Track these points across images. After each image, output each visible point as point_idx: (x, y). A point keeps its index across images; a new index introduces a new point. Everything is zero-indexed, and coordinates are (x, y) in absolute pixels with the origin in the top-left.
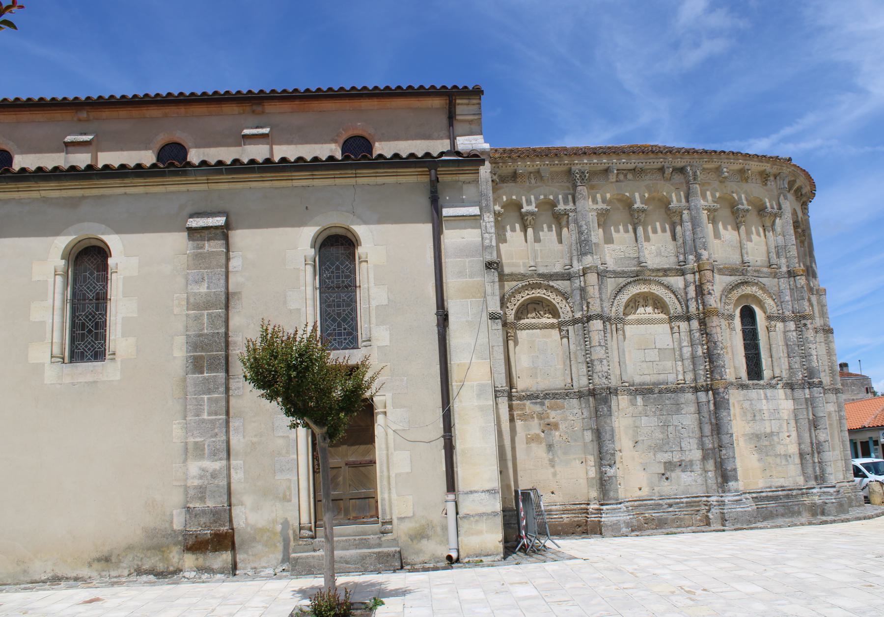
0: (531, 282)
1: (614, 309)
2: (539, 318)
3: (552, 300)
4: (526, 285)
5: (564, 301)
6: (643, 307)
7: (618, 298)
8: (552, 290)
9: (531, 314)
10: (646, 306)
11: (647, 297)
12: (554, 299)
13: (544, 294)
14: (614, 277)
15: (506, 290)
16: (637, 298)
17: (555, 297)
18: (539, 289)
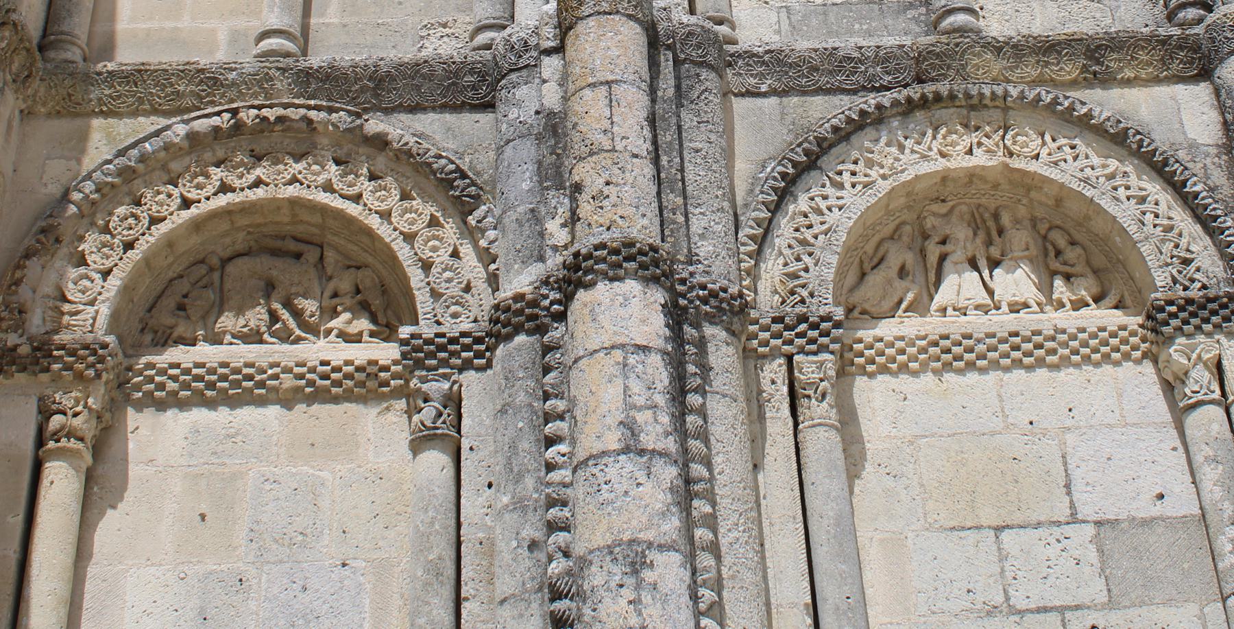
0: (247, 116)
1: (772, 269)
2: (286, 337)
3: (374, 222)
4: (216, 129)
5: (450, 230)
6: (973, 263)
7: (803, 203)
8: (381, 162)
9: (240, 311)
10: (994, 264)
11: (996, 216)
12: (386, 215)
13: (328, 188)
14: (773, 92)
15: (88, 163)
16: (930, 222)
17: (392, 200)
18: (298, 158)
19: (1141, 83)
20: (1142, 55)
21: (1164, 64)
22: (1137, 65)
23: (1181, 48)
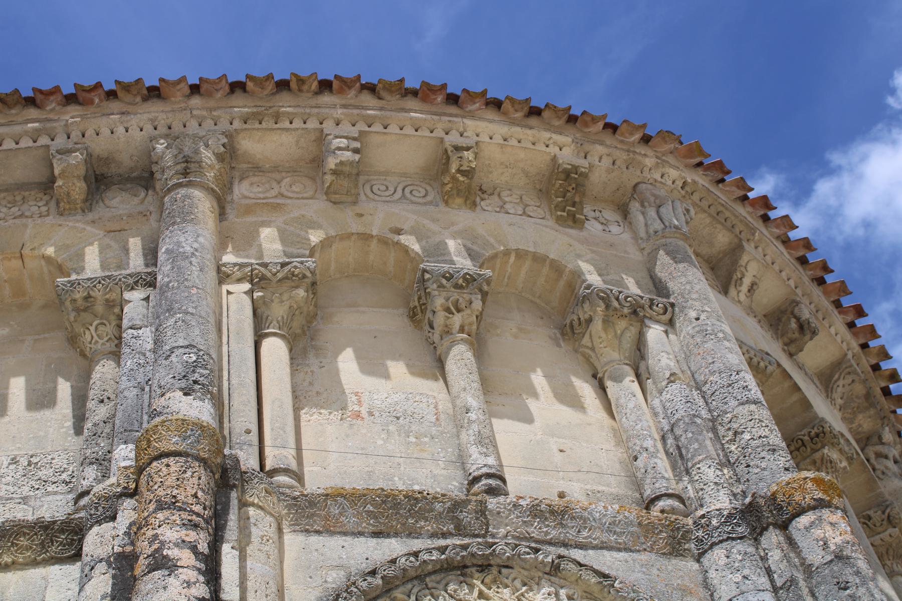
19: (19, 567)
20: (23, 542)
21: (43, 547)
22: (17, 550)
23: (62, 531)
